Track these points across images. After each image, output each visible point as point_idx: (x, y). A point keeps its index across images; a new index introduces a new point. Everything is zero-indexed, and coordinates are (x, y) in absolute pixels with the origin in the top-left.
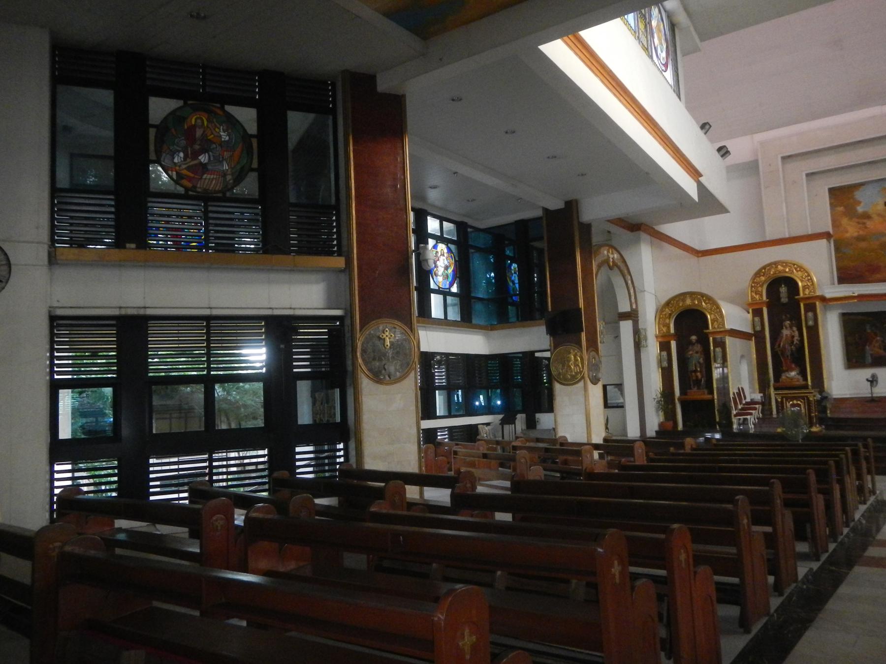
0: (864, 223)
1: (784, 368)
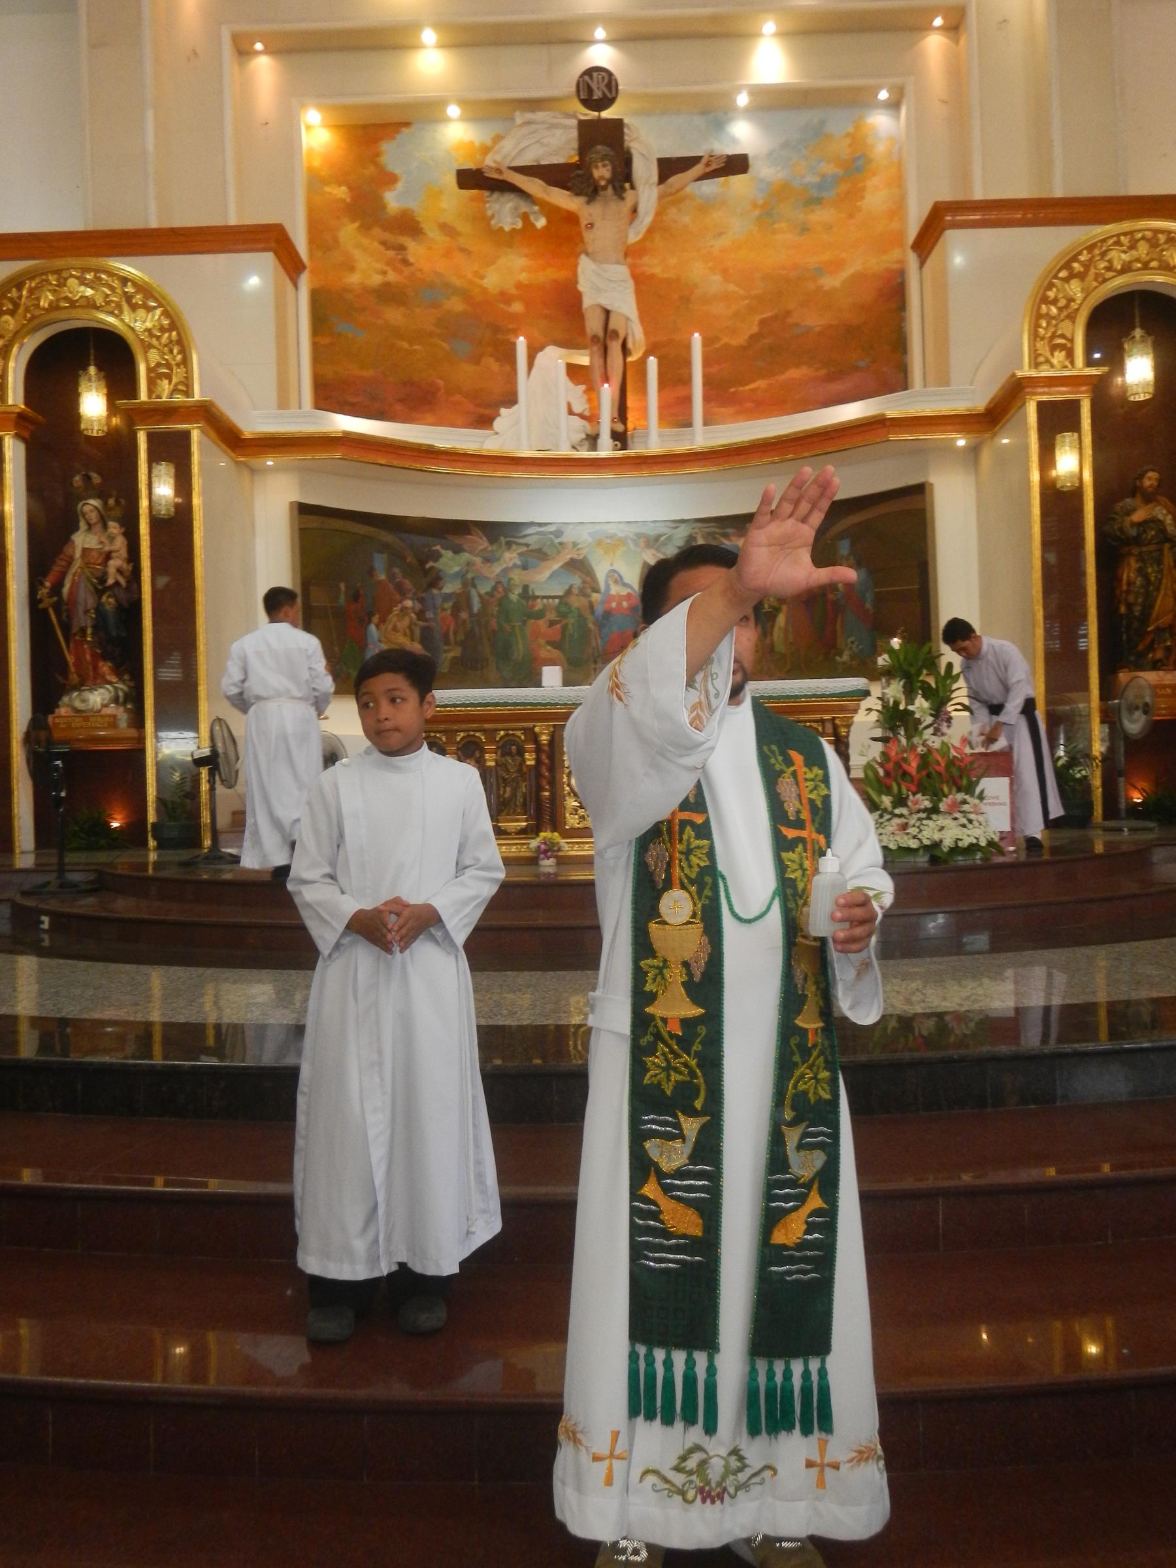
0: (402, 248)
1: (74, 678)
